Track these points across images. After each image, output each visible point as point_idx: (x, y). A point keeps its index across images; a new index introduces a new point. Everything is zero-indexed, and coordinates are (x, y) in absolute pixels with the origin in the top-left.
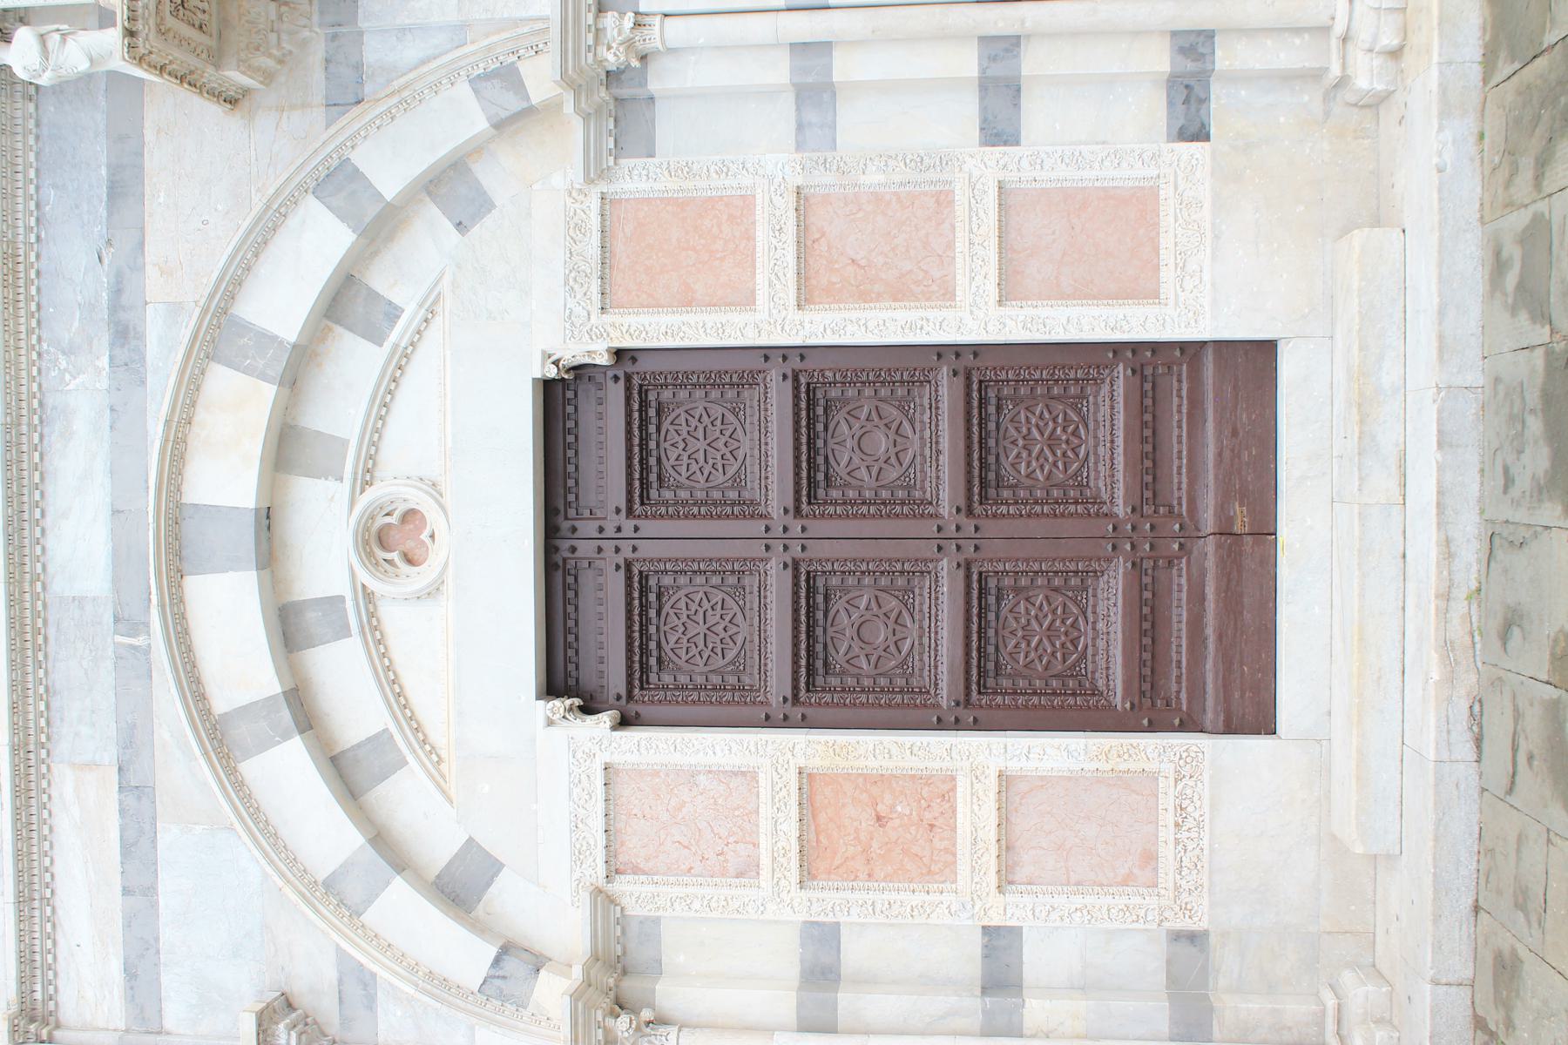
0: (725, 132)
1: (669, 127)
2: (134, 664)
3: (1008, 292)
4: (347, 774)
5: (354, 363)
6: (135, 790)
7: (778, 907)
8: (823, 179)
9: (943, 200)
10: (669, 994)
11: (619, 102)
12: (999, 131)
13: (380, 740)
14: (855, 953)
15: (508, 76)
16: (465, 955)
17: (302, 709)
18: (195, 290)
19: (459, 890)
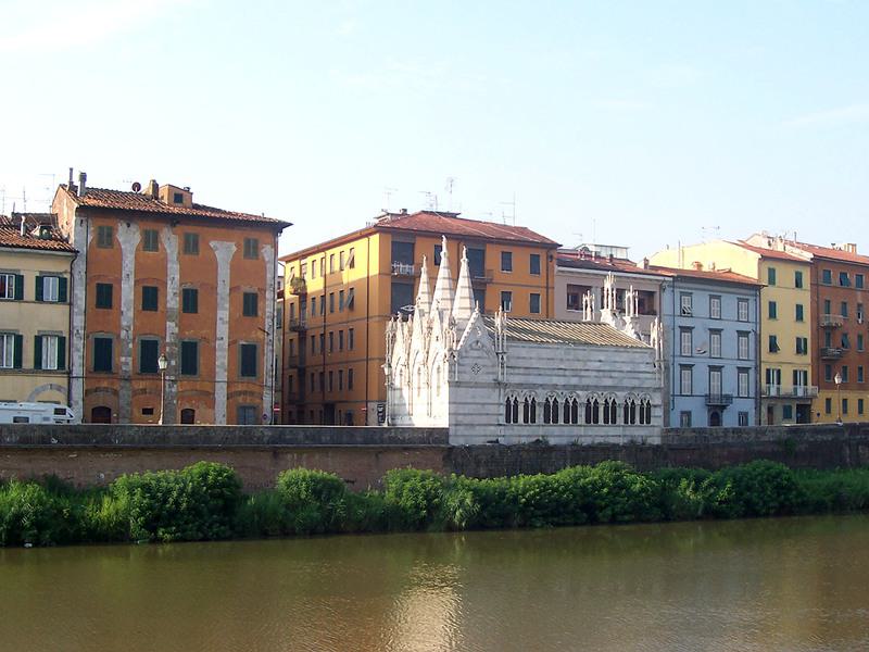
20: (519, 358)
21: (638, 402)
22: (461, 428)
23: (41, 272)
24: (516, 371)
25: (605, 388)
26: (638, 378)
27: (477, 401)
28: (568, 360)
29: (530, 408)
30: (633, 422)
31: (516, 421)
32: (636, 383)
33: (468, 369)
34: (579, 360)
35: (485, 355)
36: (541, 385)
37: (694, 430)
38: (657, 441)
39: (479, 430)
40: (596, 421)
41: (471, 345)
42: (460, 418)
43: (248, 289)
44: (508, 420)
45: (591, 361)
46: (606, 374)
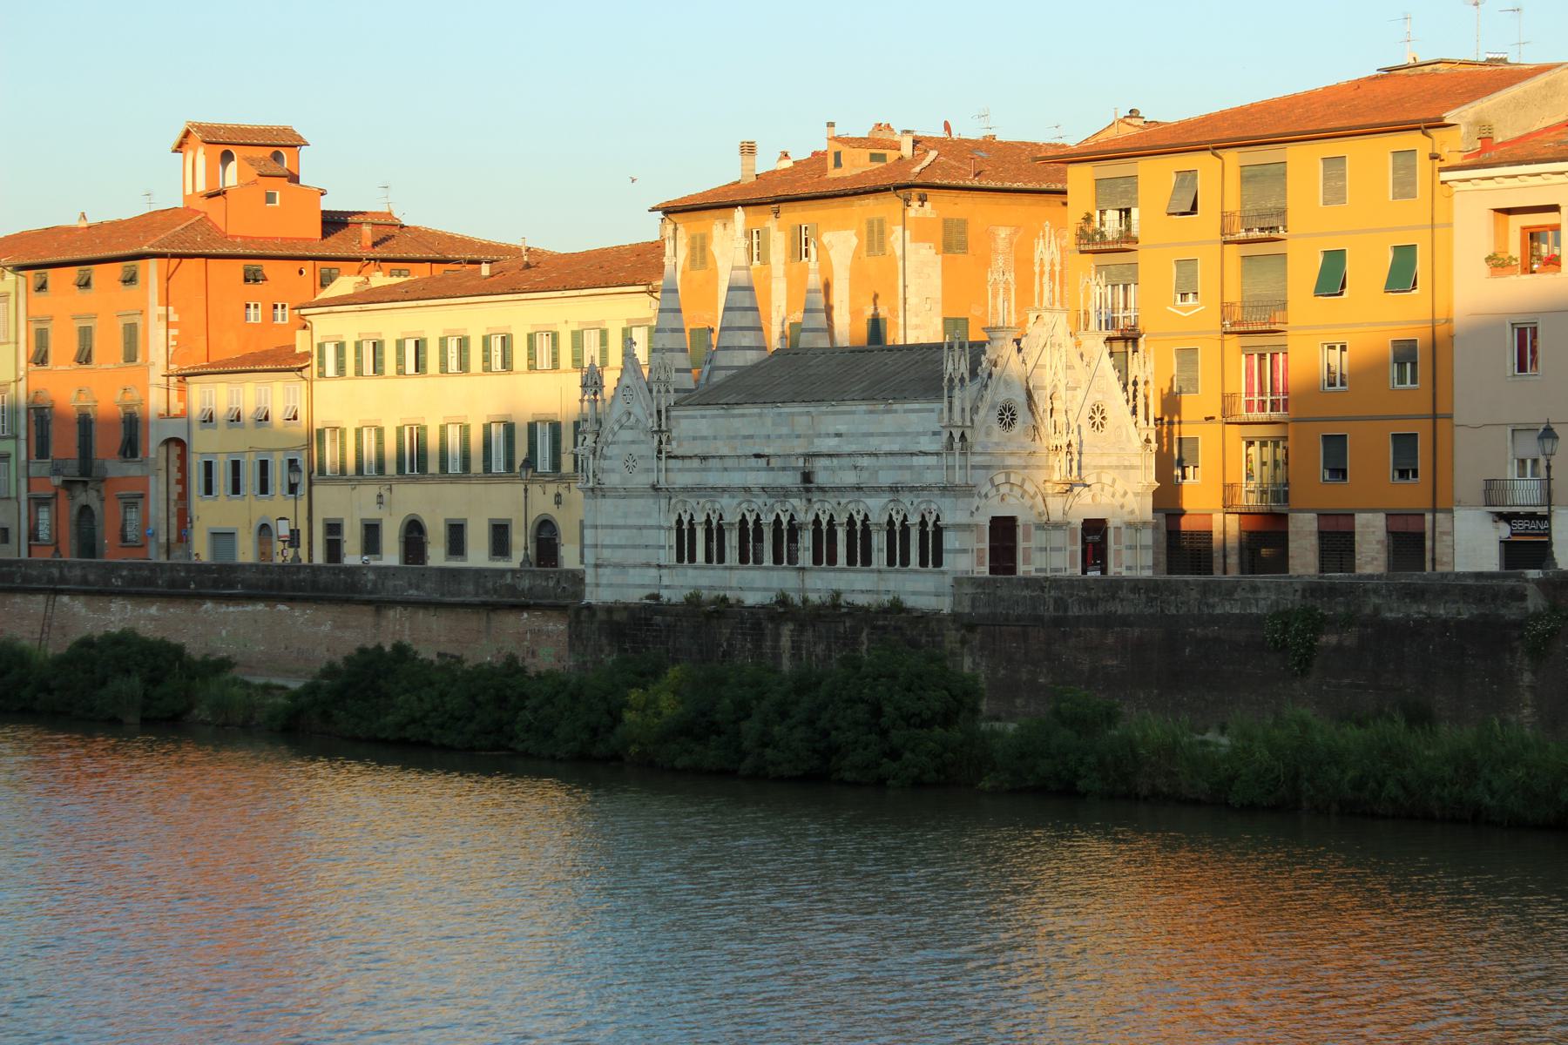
0: (1038, 539)
20: (695, 438)
21: (914, 519)
22: (607, 571)
23: (628, 321)
24: (688, 463)
25: (839, 490)
26: (910, 468)
27: (630, 522)
28: (780, 436)
29: (716, 533)
30: (905, 561)
31: (692, 559)
32: (906, 478)
33: (618, 464)
34: (798, 436)
35: (642, 437)
36: (724, 490)
37: (1029, 582)
38: (945, 605)
39: (635, 576)
40: (832, 560)
41: (618, 421)
42: (606, 553)
44: (680, 559)
45: (819, 436)
46: (846, 461)
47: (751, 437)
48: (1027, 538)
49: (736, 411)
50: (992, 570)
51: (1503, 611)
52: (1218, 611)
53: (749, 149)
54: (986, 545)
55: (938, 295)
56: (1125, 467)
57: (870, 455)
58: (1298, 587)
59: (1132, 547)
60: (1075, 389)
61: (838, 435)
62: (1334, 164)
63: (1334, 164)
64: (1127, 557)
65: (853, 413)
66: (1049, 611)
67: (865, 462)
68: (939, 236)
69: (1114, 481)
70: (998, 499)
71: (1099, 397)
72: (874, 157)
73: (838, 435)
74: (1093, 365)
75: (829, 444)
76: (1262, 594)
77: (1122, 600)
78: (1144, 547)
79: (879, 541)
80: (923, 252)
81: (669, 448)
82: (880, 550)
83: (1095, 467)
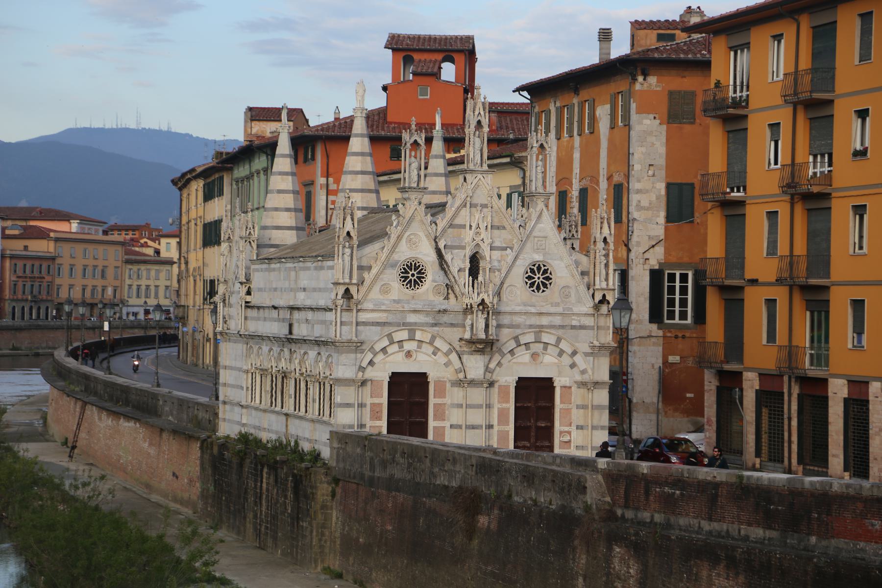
1: (456, 389)
2: (398, 325)
3: (435, 428)
4: (384, 350)
5: (431, 349)
6: (383, 324)
7: (369, 401)
8: (447, 407)
9: (444, 420)
10: (360, 389)
11: (459, 383)
12: (452, 426)
13: (387, 352)
14: (364, 409)
15: (461, 372)
16: (364, 364)
17: (392, 342)
18: (440, 334)
19: (371, 363)
36: (261, 338)
43: (617, 179)
47: (275, 289)
48: (441, 393)
49: (273, 266)
50: (392, 427)
51: (574, 505)
52: (438, 482)
53: (605, 35)
54: (384, 400)
55: (662, 162)
56: (573, 327)
57: (312, 309)
58: (474, 462)
59: (584, 407)
60: (505, 249)
61: (304, 290)
62: (866, 17)
63: (866, 17)
64: (577, 416)
65: (308, 269)
66: (368, 473)
67: (310, 315)
68: (664, 109)
69: (559, 340)
70: (401, 356)
71: (538, 257)
72: (660, 37)
73: (304, 290)
74: (529, 227)
75: (302, 299)
76: (458, 468)
77: (397, 464)
78: (599, 407)
79: (314, 391)
80: (647, 122)
81: (248, 298)
82: (314, 401)
83: (531, 326)
